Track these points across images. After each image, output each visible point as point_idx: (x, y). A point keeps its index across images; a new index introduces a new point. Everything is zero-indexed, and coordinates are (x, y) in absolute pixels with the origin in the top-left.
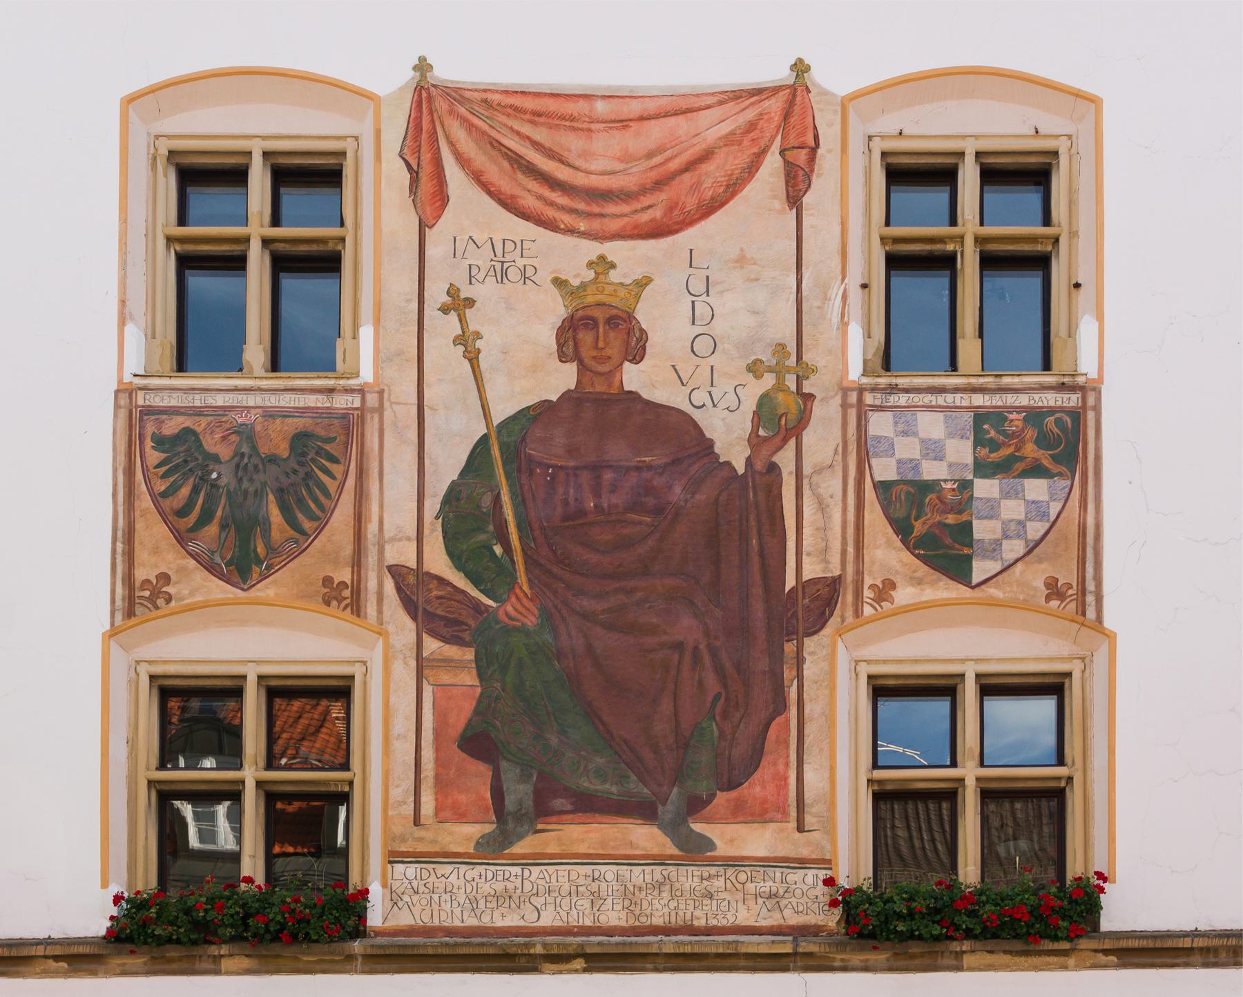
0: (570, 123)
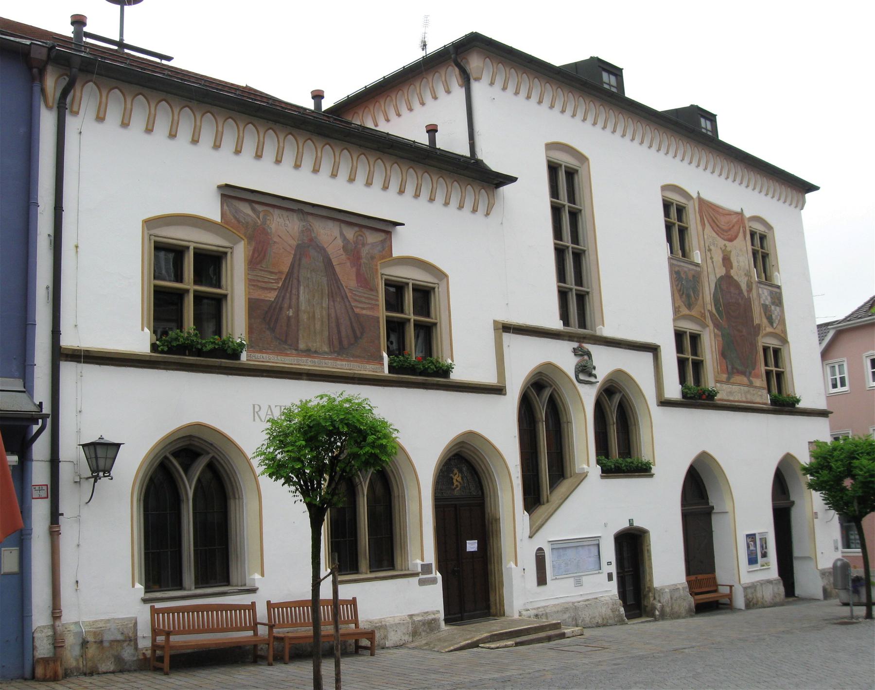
0: (718, 212)
